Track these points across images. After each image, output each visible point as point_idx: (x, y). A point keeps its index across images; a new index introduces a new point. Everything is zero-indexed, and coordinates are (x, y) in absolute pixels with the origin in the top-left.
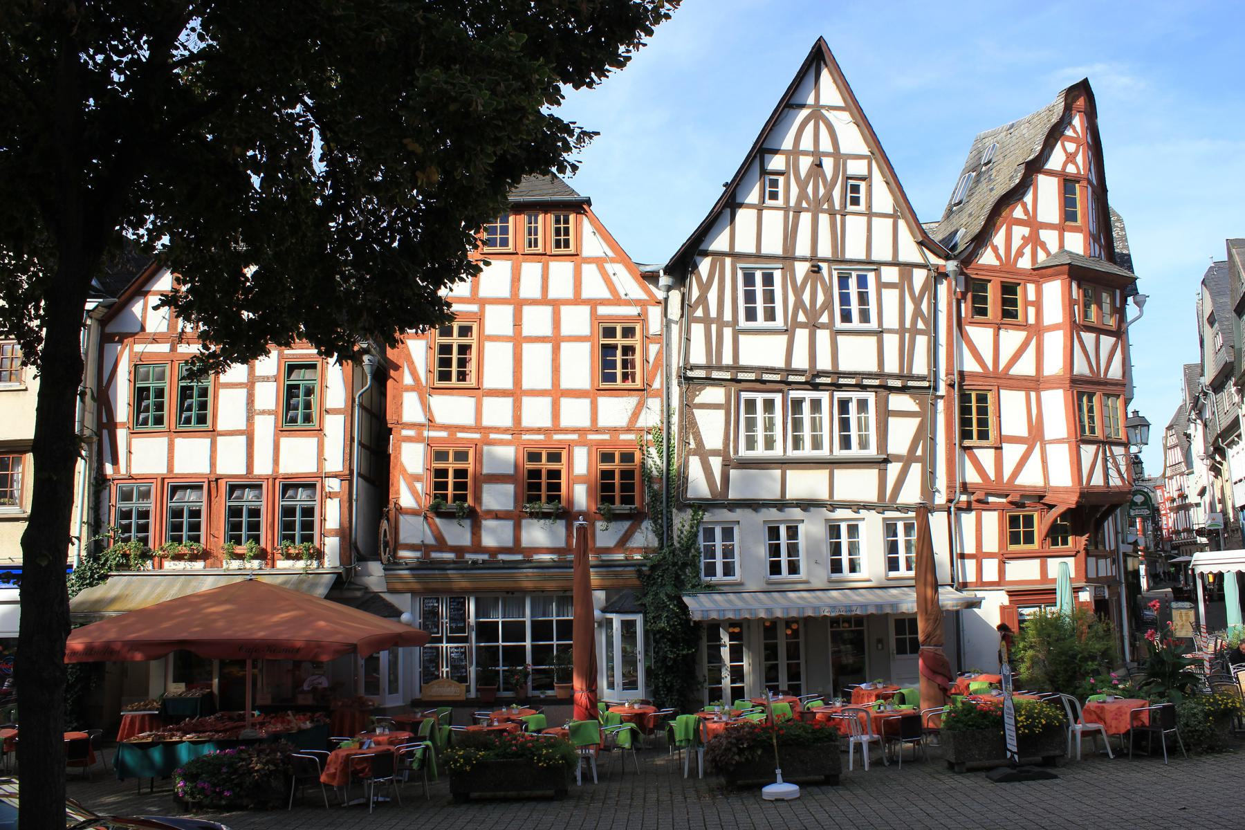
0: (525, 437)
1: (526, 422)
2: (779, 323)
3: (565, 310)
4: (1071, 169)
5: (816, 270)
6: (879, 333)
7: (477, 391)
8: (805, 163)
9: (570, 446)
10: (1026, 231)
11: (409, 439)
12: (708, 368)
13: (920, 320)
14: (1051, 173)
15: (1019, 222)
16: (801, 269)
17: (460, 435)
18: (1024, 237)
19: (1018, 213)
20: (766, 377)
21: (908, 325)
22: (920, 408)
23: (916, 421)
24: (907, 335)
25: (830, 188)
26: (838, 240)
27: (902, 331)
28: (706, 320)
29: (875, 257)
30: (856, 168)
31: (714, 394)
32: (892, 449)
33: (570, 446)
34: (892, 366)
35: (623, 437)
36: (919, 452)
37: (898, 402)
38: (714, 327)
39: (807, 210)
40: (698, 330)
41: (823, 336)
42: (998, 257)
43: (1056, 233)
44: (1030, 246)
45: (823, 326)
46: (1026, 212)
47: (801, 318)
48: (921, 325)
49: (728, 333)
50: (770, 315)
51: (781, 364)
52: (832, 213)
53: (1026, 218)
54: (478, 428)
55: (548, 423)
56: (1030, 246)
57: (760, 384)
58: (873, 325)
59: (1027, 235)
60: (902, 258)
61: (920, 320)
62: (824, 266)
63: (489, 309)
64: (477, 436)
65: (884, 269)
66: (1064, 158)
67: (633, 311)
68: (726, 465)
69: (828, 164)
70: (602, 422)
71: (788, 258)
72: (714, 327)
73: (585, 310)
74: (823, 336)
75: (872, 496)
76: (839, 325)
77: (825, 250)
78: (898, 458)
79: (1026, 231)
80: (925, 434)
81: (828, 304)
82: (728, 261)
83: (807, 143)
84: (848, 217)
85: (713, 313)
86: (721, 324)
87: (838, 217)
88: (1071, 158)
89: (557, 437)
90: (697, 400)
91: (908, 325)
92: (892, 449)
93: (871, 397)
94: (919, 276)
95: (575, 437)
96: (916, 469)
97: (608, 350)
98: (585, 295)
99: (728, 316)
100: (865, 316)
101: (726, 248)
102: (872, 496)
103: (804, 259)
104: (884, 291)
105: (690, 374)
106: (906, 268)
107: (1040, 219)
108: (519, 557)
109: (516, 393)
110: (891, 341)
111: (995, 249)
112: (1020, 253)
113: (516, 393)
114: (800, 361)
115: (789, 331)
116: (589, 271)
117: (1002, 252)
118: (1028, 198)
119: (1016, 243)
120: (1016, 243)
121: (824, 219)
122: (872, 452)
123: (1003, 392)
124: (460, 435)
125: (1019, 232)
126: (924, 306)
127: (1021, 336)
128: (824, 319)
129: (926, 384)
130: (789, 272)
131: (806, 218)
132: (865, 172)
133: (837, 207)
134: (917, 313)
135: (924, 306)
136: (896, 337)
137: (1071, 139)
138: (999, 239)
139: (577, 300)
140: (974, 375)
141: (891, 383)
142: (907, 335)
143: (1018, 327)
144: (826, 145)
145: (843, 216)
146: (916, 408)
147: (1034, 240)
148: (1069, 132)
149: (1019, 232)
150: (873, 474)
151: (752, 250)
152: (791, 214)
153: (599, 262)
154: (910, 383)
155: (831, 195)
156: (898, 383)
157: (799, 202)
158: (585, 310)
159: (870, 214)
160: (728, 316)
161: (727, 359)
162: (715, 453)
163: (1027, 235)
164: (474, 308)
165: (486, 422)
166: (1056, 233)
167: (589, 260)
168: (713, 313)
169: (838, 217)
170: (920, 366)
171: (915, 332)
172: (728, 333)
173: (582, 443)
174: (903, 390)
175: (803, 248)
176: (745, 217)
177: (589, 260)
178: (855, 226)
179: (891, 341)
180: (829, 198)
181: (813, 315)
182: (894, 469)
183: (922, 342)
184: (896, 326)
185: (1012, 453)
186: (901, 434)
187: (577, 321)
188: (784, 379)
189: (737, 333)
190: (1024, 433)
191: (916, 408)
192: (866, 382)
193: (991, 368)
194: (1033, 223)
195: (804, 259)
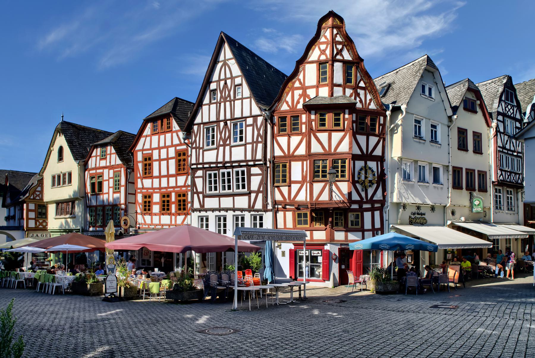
0: (162, 190)
1: (162, 186)
2: (215, 146)
3: (169, 149)
4: (323, 58)
5: (226, 124)
6: (245, 145)
7: (152, 177)
8: (222, 83)
9: (171, 192)
10: (300, 92)
11: (139, 193)
12: (196, 164)
13: (259, 138)
14: (312, 62)
15: (298, 88)
16: (222, 124)
17: (149, 191)
18: (300, 95)
19: (297, 84)
20: (212, 165)
21: (255, 140)
22: (262, 172)
23: (260, 177)
24: (255, 144)
25: (229, 92)
26: (232, 112)
27: (252, 143)
28: (196, 148)
29: (244, 116)
30: (238, 81)
31: (199, 173)
32: (252, 189)
33: (171, 192)
34: (249, 157)
35: (183, 189)
36: (261, 189)
37: (255, 170)
38: (198, 150)
39: (222, 102)
40: (194, 151)
41: (227, 148)
42: (289, 106)
43: (314, 90)
44: (302, 98)
45: (228, 145)
46: (300, 83)
47: (221, 143)
48: (260, 139)
49: (201, 151)
50: (213, 143)
51: (215, 161)
52: (230, 101)
53: (300, 86)
54: (152, 188)
55: (166, 186)
56: (302, 98)
57: (211, 169)
58: (243, 142)
59: (301, 93)
60: (253, 114)
61: (259, 138)
62: (228, 122)
63: (154, 151)
64: (152, 191)
65: (248, 119)
66: (319, 53)
67: (184, 147)
68: (204, 197)
69: (229, 82)
70: (179, 184)
71: (218, 121)
72: (198, 150)
73: (174, 148)
74: (227, 148)
75: (246, 206)
76: (233, 144)
77: (228, 116)
78: (254, 192)
79: (300, 92)
80: (263, 183)
81: (229, 137)
82: (202, 125)
83: (222, 77)
84: (236, 102)
85: (198, 146)
86: (200, 148)
87: (232, 102)
88: (323, 52)
89: (169, 190)
90: (196, 175)
91: (255, 140)
92: (252, 189)
93: (245, 169)
94: (260, 120)
95: (172, 189)
96: (260, 195)
97: (180, 161)
98: (174, 143)
99: (201, 146)
100: (241, 139)
101: (200, 122)
102: (246, 206)
103: (222, 121)
104: (248, 128)
105: (192, 167)
106: (255, 117)
107: (307, 84)
108: (160, 227)
109: (160, 177)
110: (249, 147)
111: (287, 103)
112: (298, 102)
113: (160, 177)
114: (220, 159)
115: (217, 148)
116: (174, 134)
117: (290, 104)
118: (301, 76)
119: (296, 98)
120: (296, 98)
121: (228, 104)
122: (246, 190)
123: (292, 163)
124: (149, 191)
125: (297, 93)
126: (261, 132)
127: (300, 138)
128: (228, 142)
129: (261, 162)
130: (219, 126)
131: (222, 104)
132: (240, 82)
133: (232, 98)
134: (259, 135)
135: (261, 132)
136: (251, 145)
137: (323, 43)
138: (289, 98)
139: (172, 146)
140: (280, 157)
141: (250, 163)
142: (255, 144)
143: (298, 134)
144: (228, 75)
145: (234, 101)
146: (260, 172)
147: (304, 95)
148: (323, 39)
149: (297, 93)
150: (246, 198)
151: (207, 121)
152: (218, 104)
153: (176, 132)
154: (257, 163)
155: (230, 94)
156: (252, 163)
157: (220, 100)
158: (174, 148)
159: (242, 99)
160: (201, 146)
161: (201, 161)
162: (201, 193)
163: (301, 93)
164: (150, 152)
165: (154, 186)
166: (314, 90)
167: (174, 132)
168: (198, 146)
169: (232, 102)
170: (259, 156)
171: (257, 142)
172: (201, 151)
173: (173, 191)
174: (255, 165)
175: (222, 117)
176: (205, 108)
177: (174, 132)
178: (238, 103)
179: (249, 147)
180: (229, 95)
181: (225, 141)
182: (253, 195)
183: (260, 146)
184: (251, 141)
185: (295, 188)
186: (255, 182)
187: (172, 152)
188: (216, 166)
189: (203, 151)
190: (300, 179)
191: (260, 172)
192: (241, 164)
193: (287, 153)
194: (304, 88)
195: (222, 121)
